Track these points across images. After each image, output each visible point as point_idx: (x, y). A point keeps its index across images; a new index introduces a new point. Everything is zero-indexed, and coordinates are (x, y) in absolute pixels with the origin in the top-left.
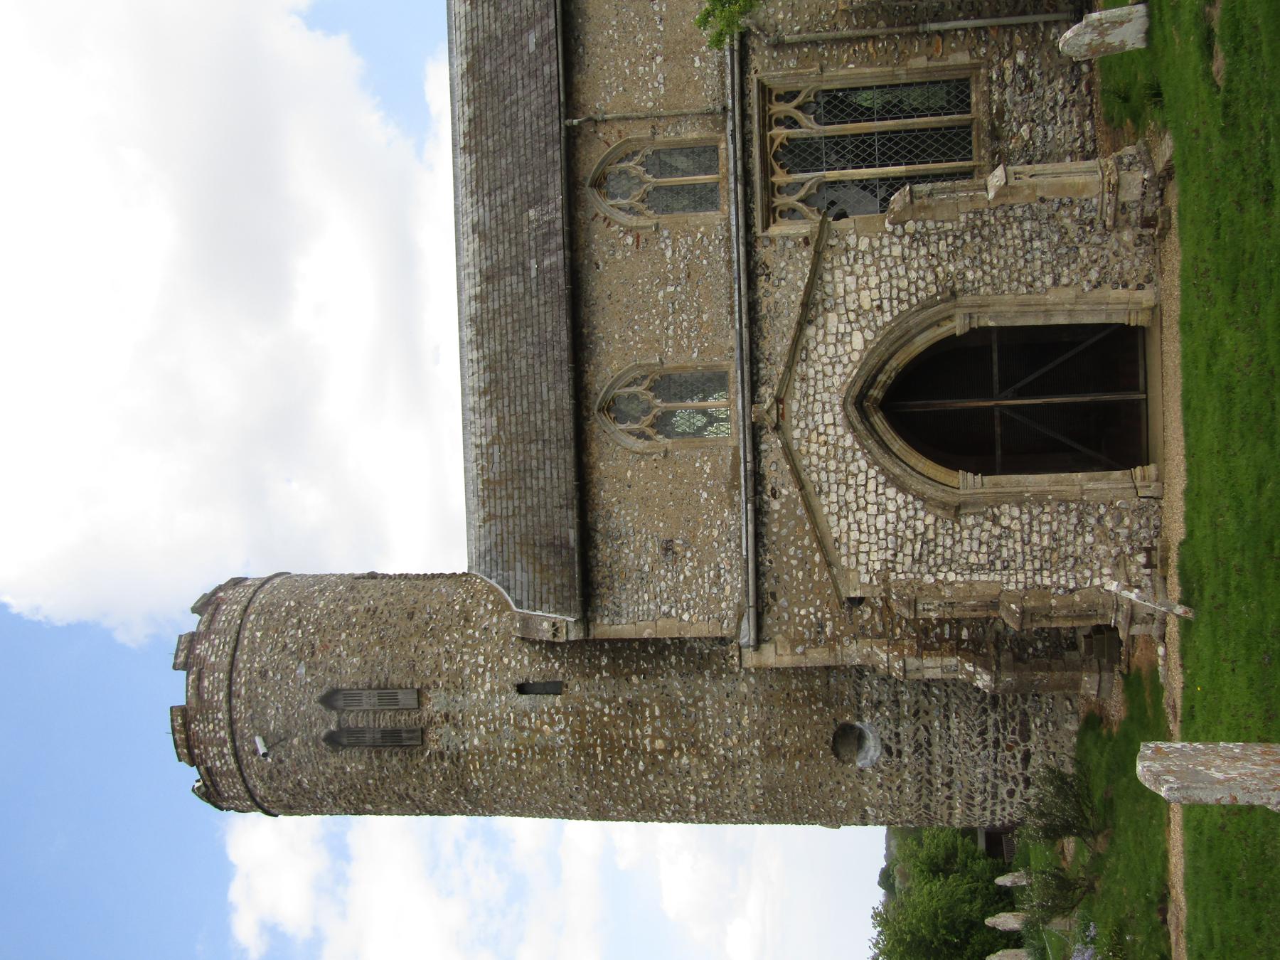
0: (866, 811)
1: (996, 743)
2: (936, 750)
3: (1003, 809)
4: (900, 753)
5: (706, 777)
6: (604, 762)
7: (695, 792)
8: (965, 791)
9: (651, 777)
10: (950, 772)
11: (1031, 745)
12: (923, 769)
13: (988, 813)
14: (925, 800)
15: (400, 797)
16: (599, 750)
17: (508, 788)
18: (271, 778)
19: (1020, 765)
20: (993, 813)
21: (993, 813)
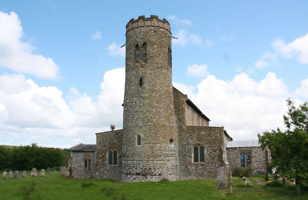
0: (158, 144)
1: (173, 169)
2: (172, 158)
3: (160, 171)
4: (171, 151)
5: (167, 114)
6: (169, 96)
7: (163, 111)
8: (165, 163)
9: (166, 104)
10: (169, 160)
11: (172, 175)
12: (169, 155)
13: (159, 168)
14: (162, 156)
15: (159, 54)
16: (170, 96)
17: (162, 76)
18: (164, 33)
19: (170, 173)
20: (158, 169)
21: (158, 169)
